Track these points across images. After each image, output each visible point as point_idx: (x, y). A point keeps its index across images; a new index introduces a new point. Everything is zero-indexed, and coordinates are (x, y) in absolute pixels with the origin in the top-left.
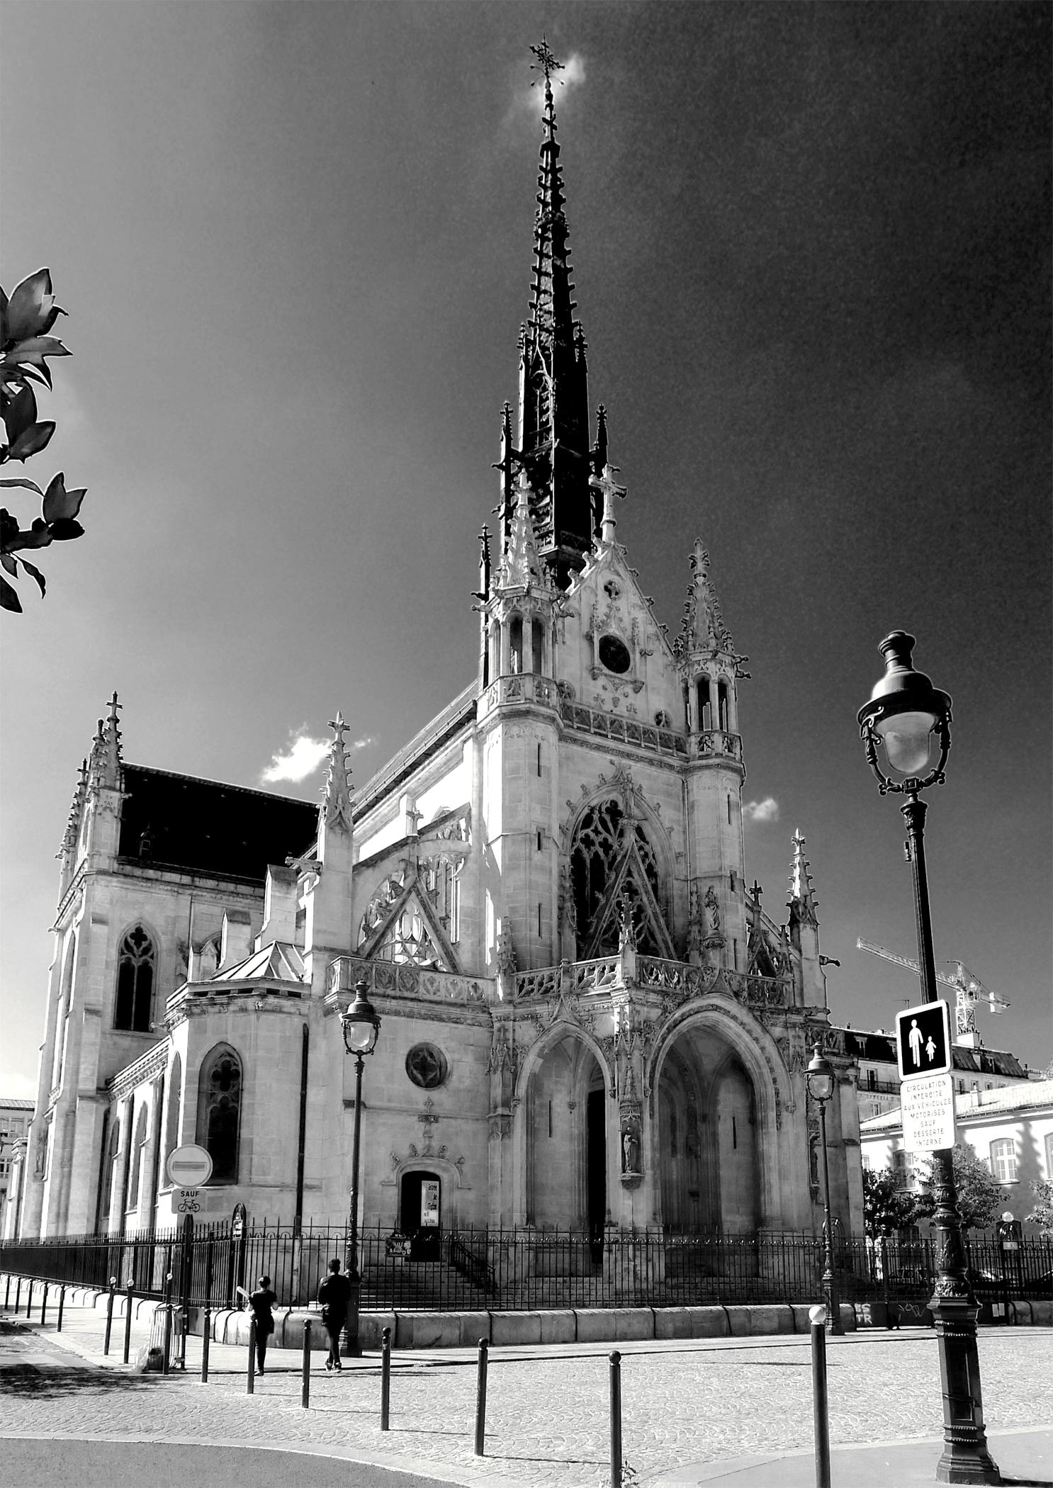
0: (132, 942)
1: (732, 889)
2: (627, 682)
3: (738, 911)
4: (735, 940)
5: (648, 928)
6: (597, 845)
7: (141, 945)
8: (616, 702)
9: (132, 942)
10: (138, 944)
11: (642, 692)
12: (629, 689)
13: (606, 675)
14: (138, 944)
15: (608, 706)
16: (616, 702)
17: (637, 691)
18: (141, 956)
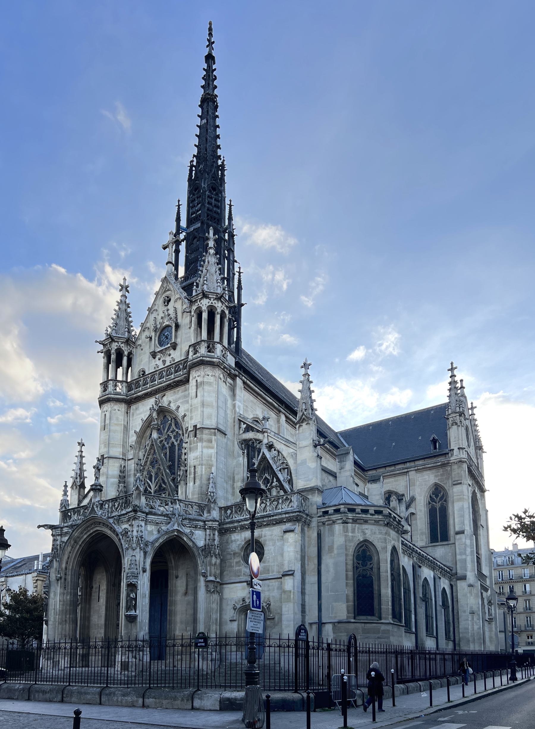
0: (434, 497)
1: (195, 436)
2: (169, 347)
3: (197, 448)
4: (195, 467)
5: (162, 479)
6: (173, 439)
7: (438, 496)
8: (164, 362)
9: (434, 497)
10: (437, 496)
11: (178, 348)
12: (172, 352)
13: (159, 352)
14: (437, 496)
15: (161, 366)
16: (164, 362)
17: (175, 349)
18: (439, 502)
